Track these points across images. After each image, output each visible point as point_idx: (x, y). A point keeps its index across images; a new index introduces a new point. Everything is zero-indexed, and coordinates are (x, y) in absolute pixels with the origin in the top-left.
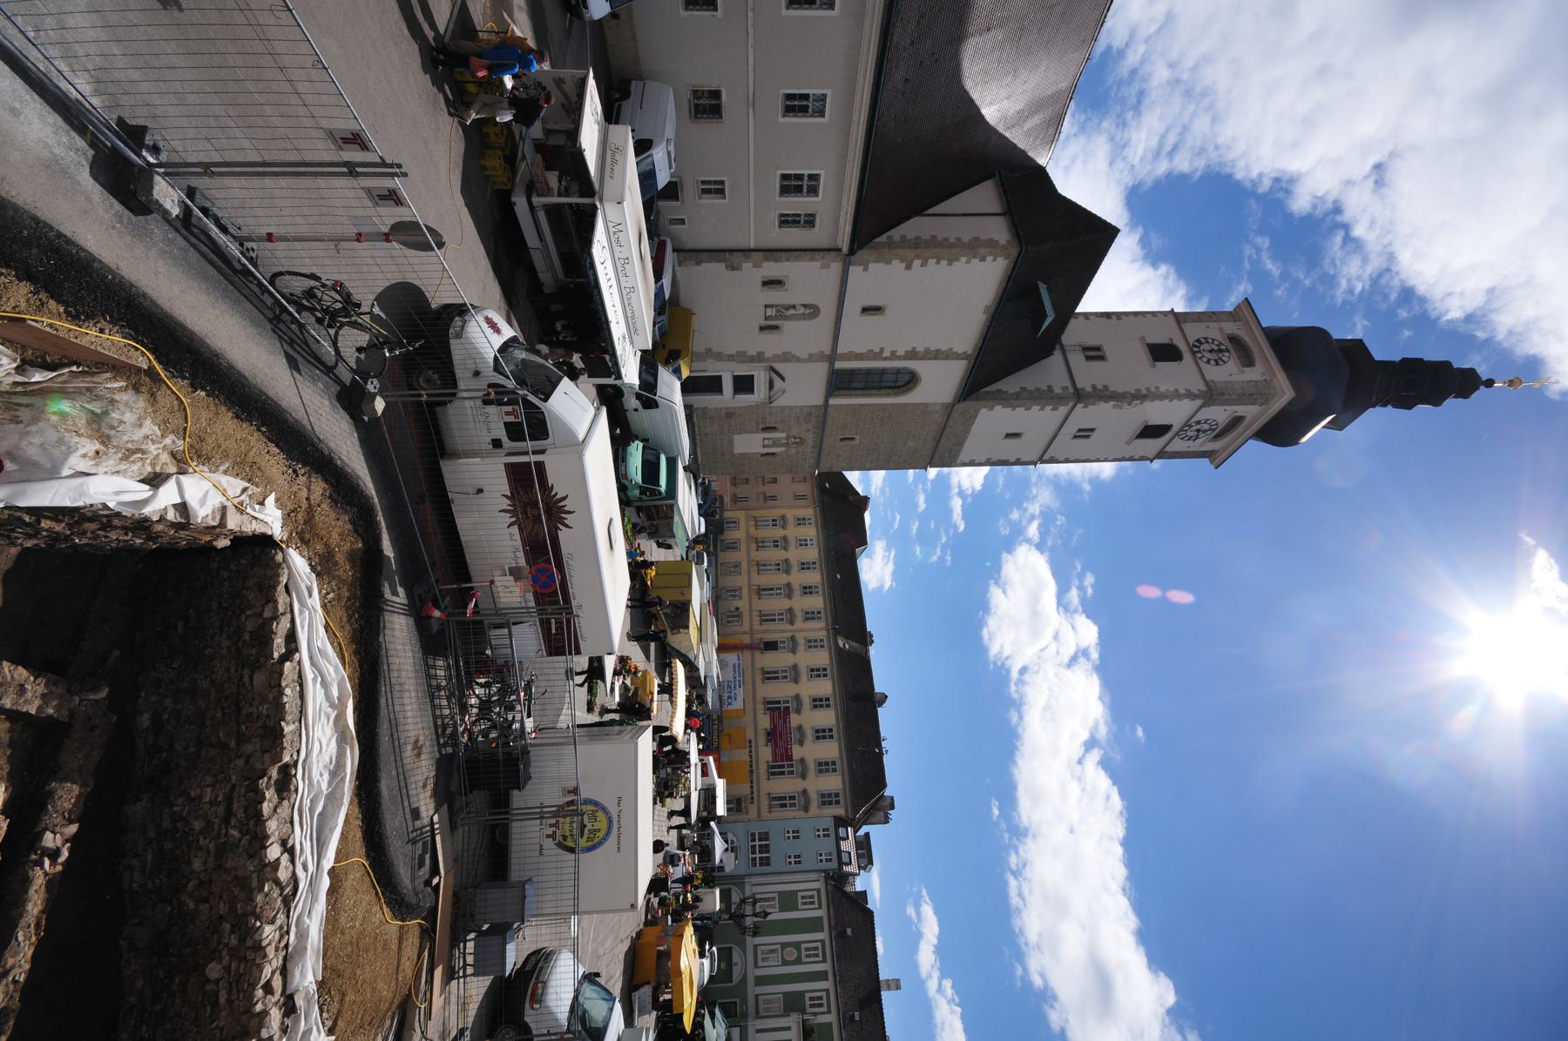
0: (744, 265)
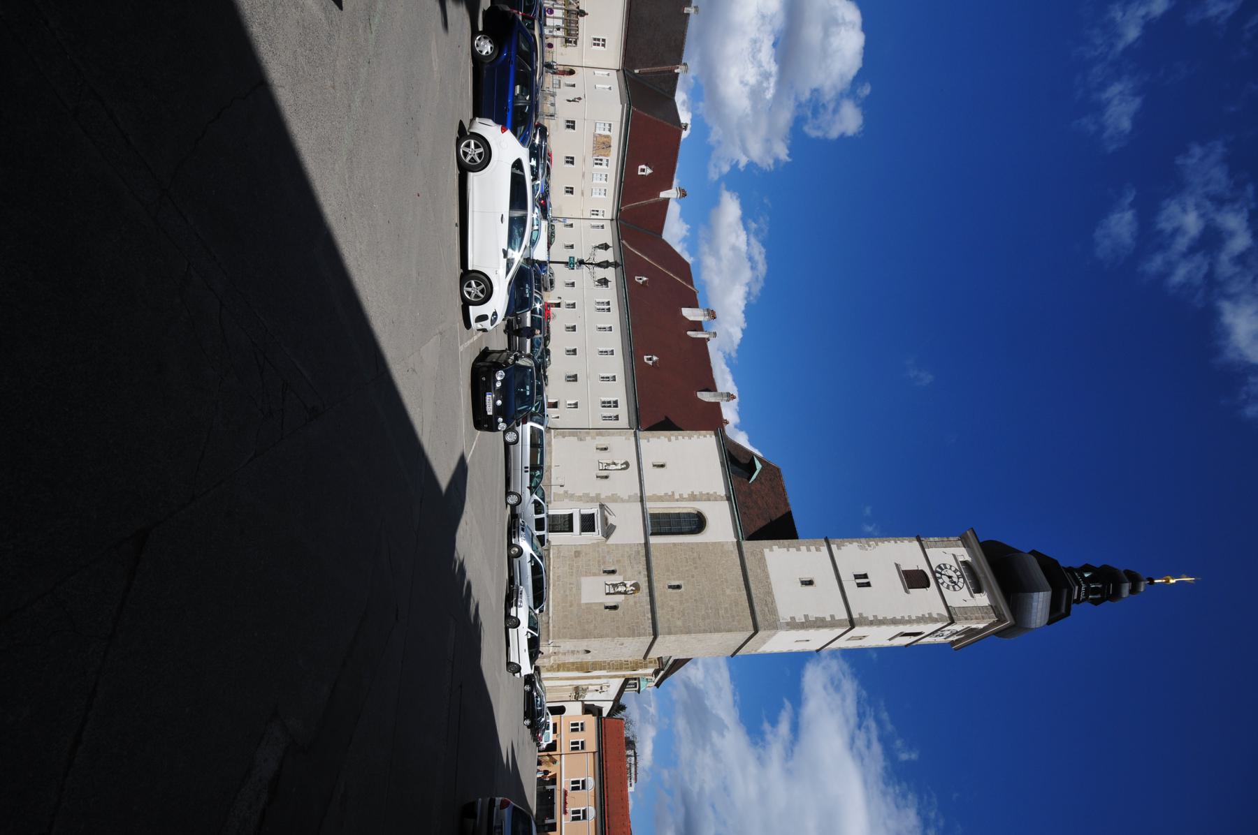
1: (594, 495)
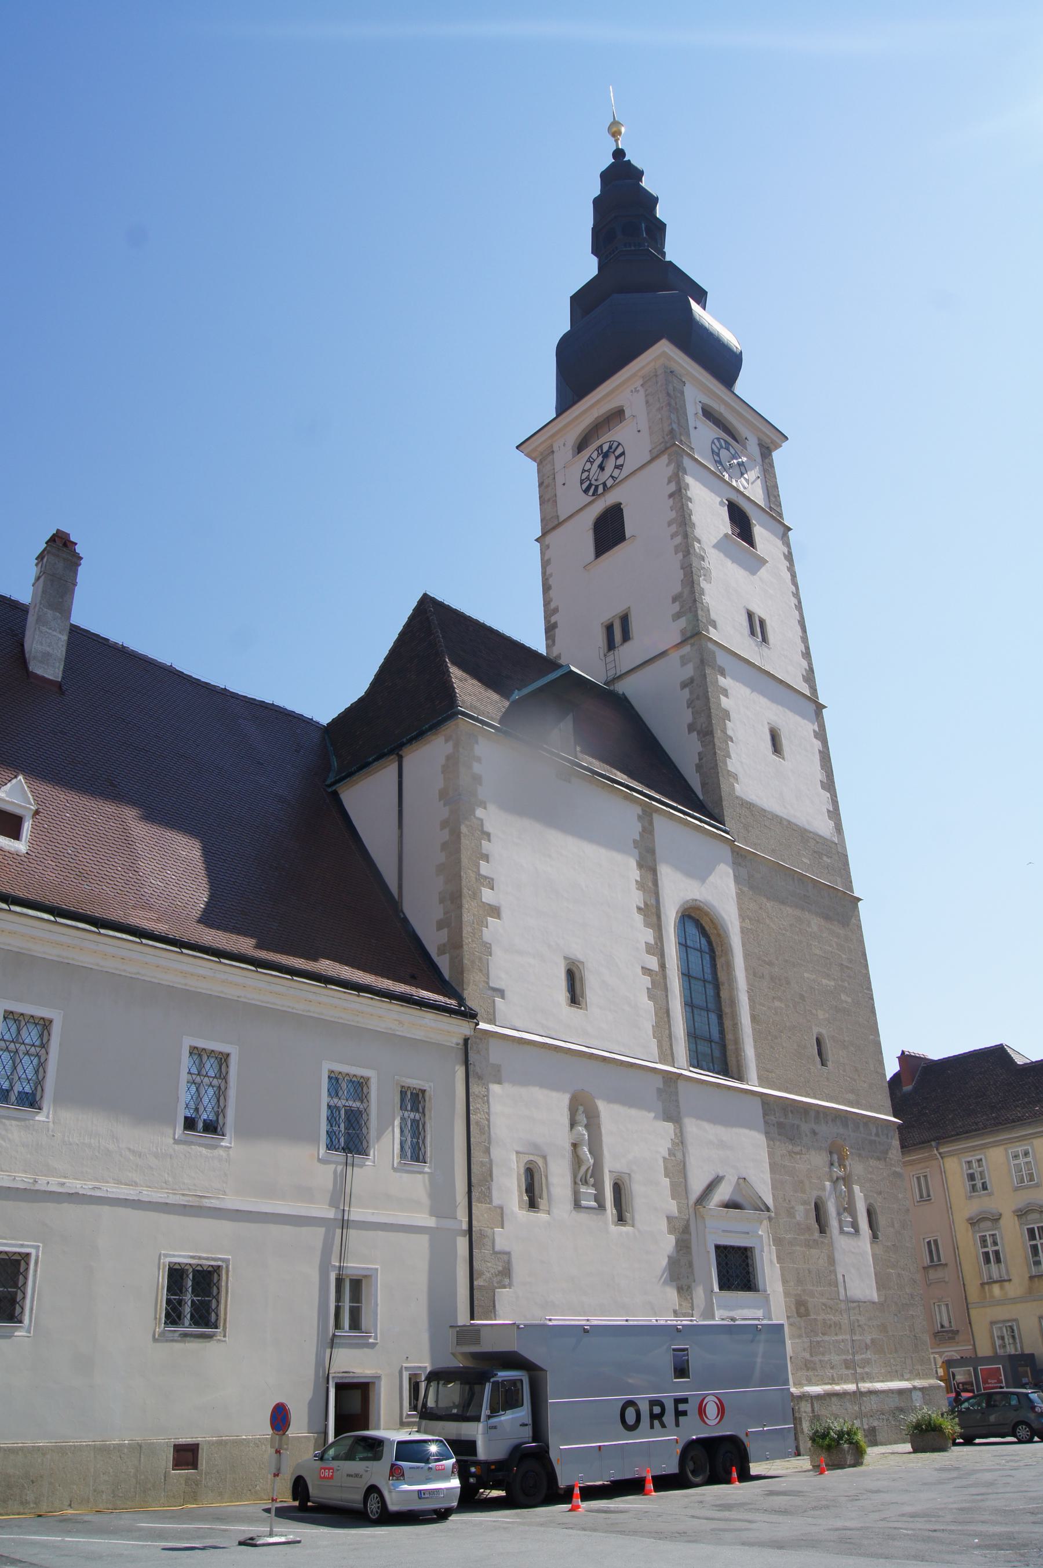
0: (500, 1244)
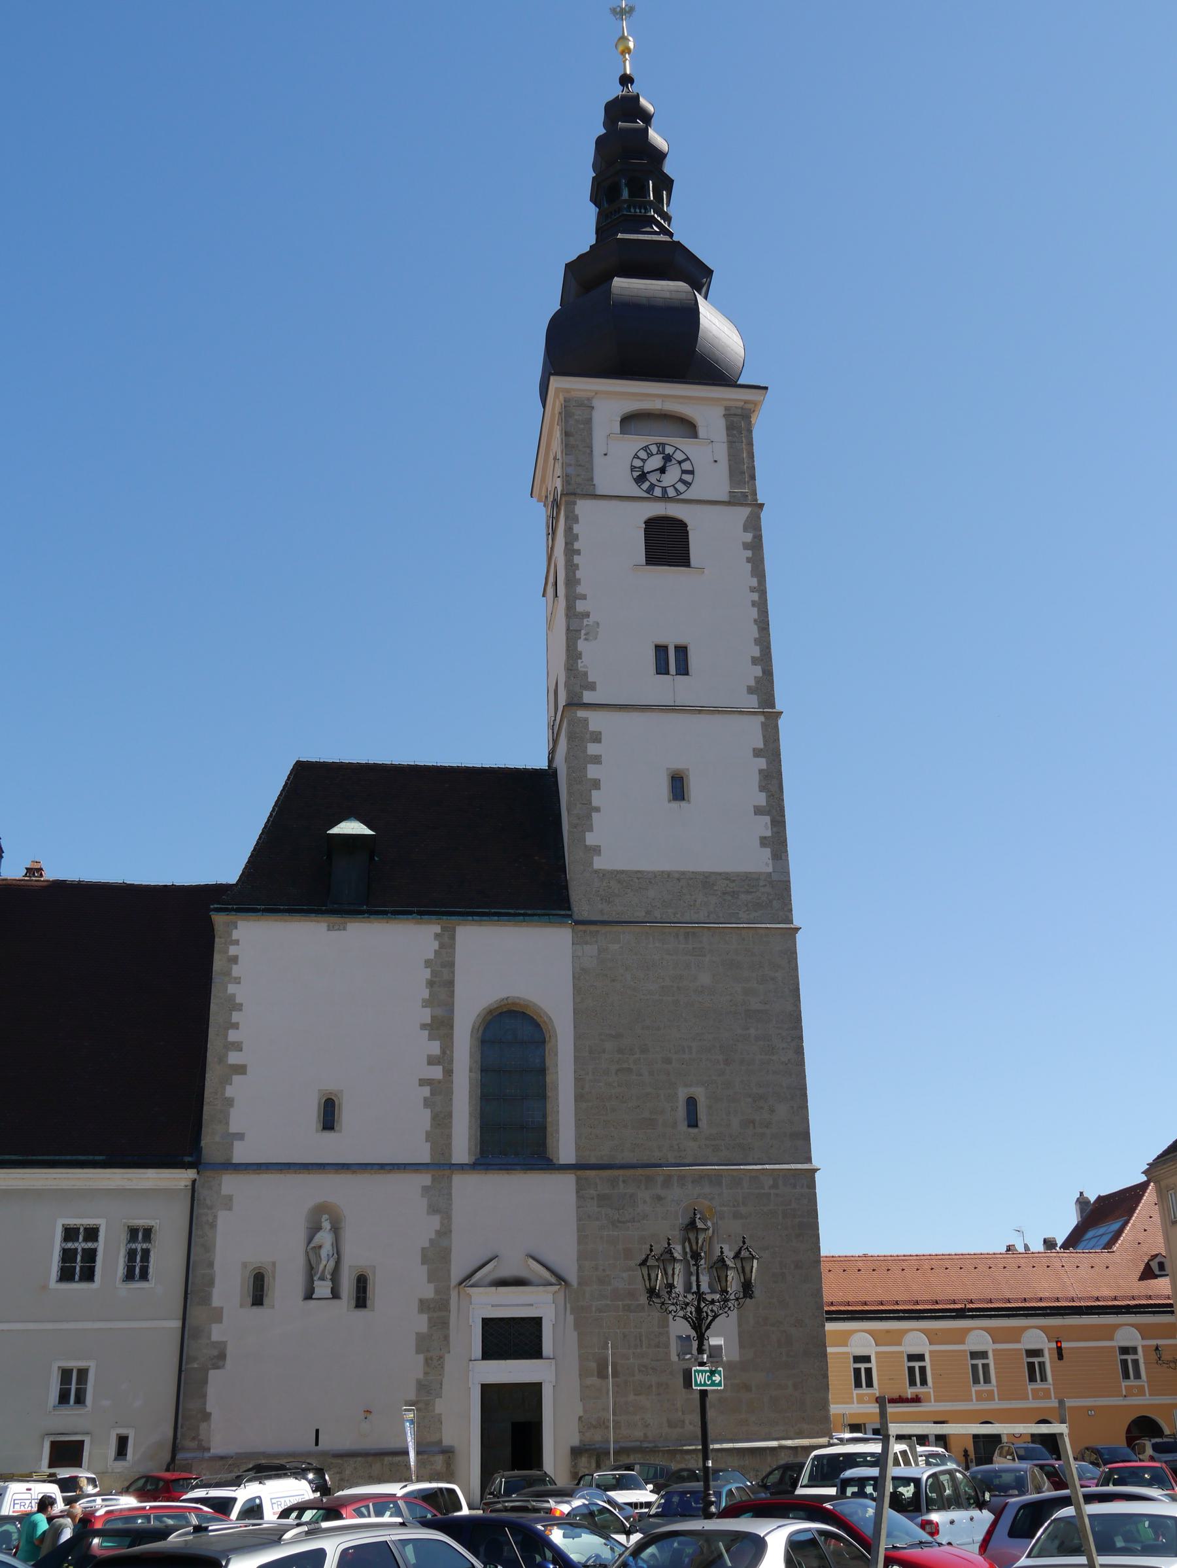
0: (215, 1337)
1: (424, 1318)
